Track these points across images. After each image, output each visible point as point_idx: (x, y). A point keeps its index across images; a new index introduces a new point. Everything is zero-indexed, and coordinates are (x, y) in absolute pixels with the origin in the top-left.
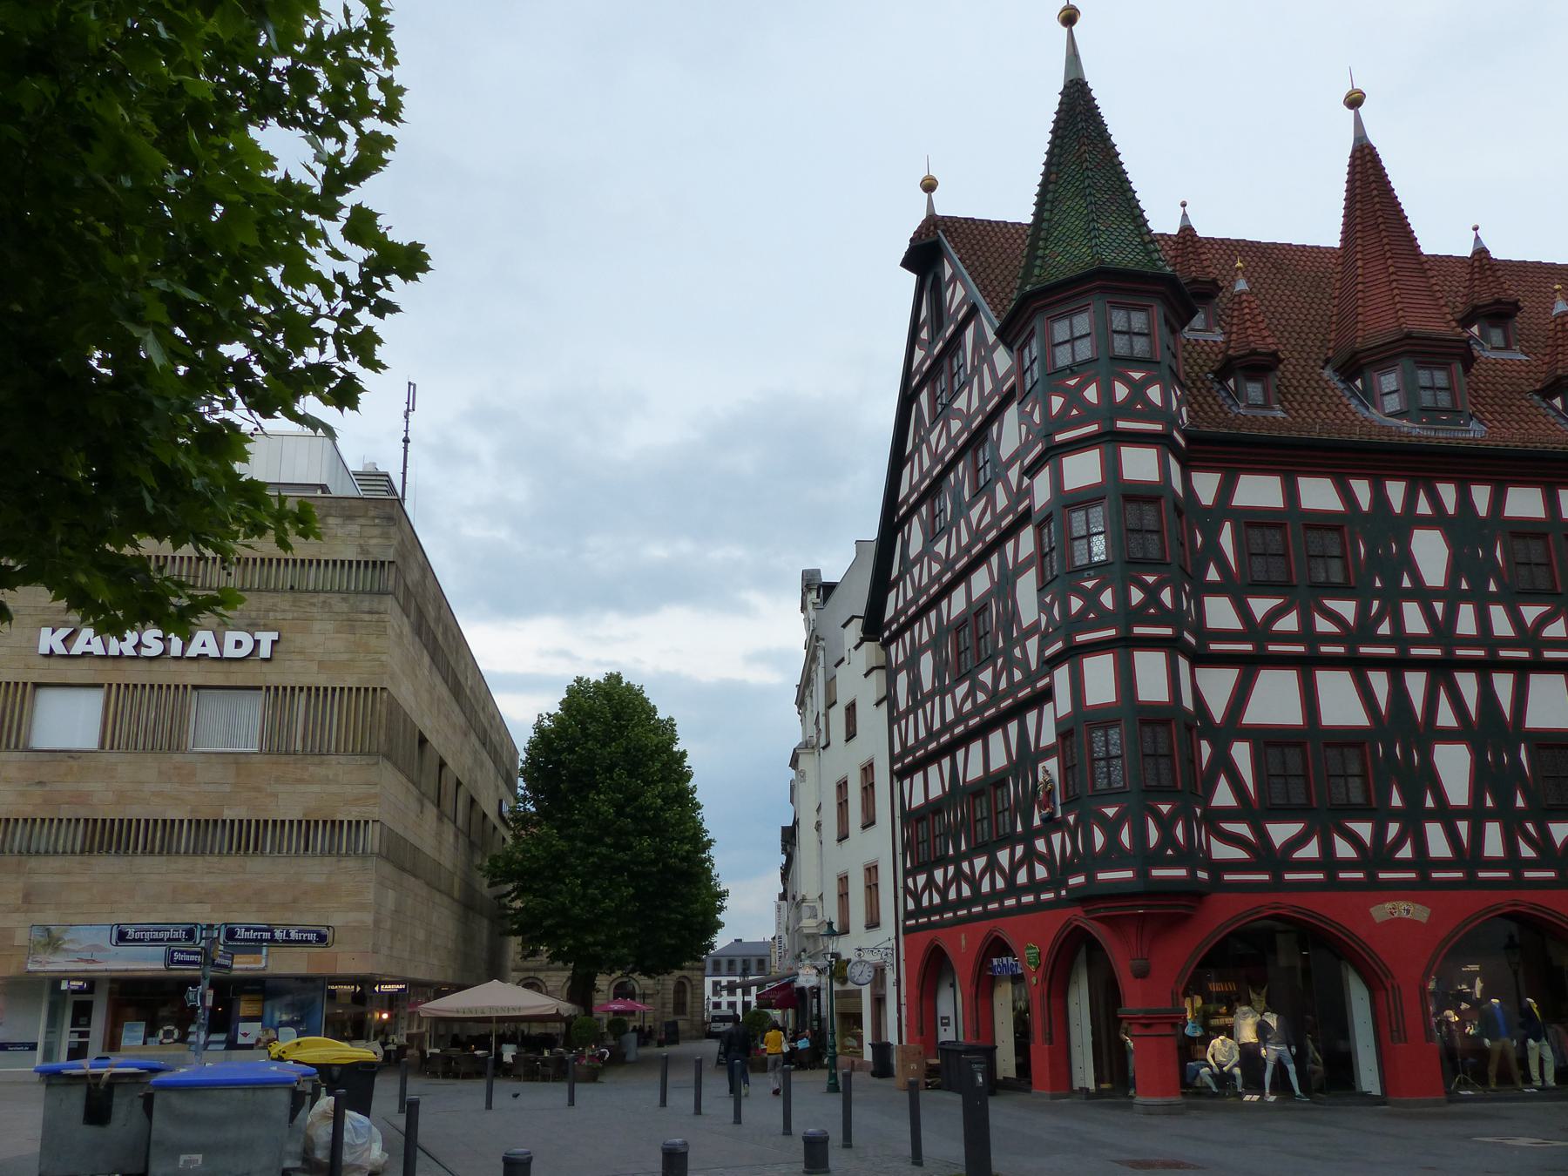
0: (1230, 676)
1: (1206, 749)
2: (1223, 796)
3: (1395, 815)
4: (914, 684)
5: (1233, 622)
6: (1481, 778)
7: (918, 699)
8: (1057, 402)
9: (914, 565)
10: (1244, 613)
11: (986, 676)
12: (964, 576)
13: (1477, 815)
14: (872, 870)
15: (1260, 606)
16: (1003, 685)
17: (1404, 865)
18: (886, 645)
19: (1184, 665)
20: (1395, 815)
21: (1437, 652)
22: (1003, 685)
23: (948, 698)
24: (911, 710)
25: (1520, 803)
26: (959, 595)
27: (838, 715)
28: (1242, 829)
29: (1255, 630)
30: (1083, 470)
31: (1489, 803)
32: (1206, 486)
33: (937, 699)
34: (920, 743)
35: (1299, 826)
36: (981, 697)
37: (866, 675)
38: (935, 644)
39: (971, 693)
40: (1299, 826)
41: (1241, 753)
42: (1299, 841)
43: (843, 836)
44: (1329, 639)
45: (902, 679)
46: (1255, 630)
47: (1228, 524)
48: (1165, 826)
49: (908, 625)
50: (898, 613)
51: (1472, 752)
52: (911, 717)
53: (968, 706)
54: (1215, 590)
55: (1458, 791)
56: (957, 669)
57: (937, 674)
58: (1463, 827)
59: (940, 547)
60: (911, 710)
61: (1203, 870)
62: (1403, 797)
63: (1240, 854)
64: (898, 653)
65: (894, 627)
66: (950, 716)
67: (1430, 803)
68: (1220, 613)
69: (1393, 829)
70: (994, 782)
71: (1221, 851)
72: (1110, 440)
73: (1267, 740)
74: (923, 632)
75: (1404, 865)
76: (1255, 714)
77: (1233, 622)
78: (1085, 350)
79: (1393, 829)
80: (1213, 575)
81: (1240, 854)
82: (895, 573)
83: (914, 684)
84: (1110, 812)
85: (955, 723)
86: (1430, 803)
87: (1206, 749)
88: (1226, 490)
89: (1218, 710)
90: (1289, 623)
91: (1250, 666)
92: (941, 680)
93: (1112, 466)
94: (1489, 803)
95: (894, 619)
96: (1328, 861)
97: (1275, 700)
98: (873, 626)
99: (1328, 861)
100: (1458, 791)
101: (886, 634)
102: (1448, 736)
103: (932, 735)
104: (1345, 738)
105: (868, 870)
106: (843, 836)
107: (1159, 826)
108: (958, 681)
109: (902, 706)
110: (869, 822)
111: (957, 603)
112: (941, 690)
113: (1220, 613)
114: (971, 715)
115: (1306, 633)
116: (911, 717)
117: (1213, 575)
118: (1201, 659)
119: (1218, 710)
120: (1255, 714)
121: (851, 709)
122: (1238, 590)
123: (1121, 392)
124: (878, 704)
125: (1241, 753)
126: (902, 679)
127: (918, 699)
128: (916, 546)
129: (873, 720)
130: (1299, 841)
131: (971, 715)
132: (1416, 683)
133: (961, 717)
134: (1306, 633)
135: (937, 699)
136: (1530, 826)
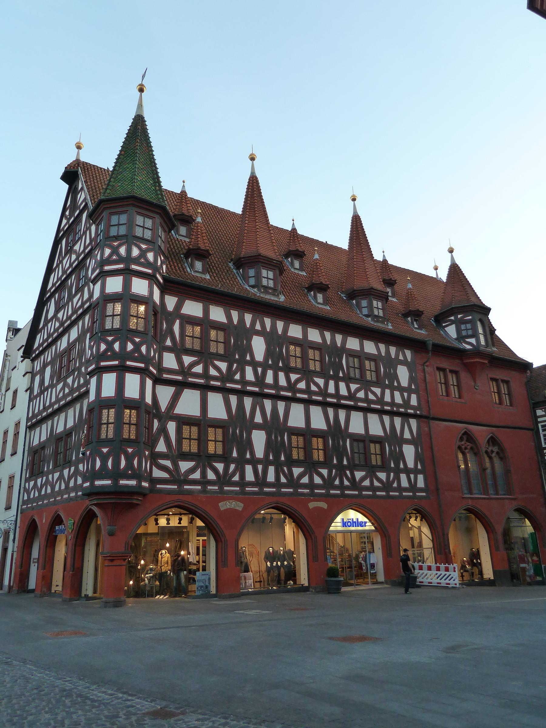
0: (171, 390)
2: (161, 447)
4: (42, 381)
7: (43, 390)
8: (108, 251)
9: (49, 322)
10: (180, 361)
11: (70, 380)
12: (67, 330)
13: (266, 463)
16: (76, 385)
18: (33, 360)
19: (149, 383)
21: (257, 389)
22: (76, 385)
23: (54, 389)
24: (42, 392)
25: (283, 458)
26: (65, 339)
27: (10, 394)
28: (168, 463)
29: (184, 371)
30: (114, 285)
31: (271, 458)
32: (171, 302)
33: (50, 390)
34: (40, 412)
36: (67, 390)
37: (24, 376)
38: (52, 363)
39: (63, 389)
41: (172, 427)
44: (215, 378)
45: (37, 379)
49: (42, 353)
50: (40, 345)
52: (38, 398)
53: (61, 395)
54: (169, 350)
56: (59, 376)
57: (52, 378)
58: (260, 467)
59: (60, 315)
60: (42, 392)
61: (145, 481)
63: (165, 475)
64: (38, 365)
65: (37, 352)
66: (53, 399)
68: (170, 361)
70: (68, 434)
71: (157, 473)
72: (128, 274)
73: (184, 421)
74: (48, 356)
75: (235, 484)
76: (179, 410)
80: (168, 343)
81: (165, 475)
82: (41, 325)
83: (42, 381)
85: (55, 403)
87: (156, 423)
90: (199, 369)
92: (53, 381)
93: (127, 285)
94: (271, 458)
95: (38, 348)
98: (28, 352)
101: (34, 355)
102: (258, 427)
103: (45, 408)
104: (216, 424)
108: (58, 382)
109: (35, 393)
111: (63, 344)
112: (52, 386)
113: (170, 361)
114: (62, 399)
115: (205, 375)
116: (38, 398)
117: (168, 343)
118: (158, 381)
120: (179, 410)
121: (15, 392)
122: (179, 350)
123: (135, 252)
124: (26, 391)
125: (172, 427)
126: (37, 379)
127: (43, 390)
128: (51, 314)
129: (23, 398)
131: (62, 399)
132: (248, 402)
133: (58, 400)
134: (205, 375)
135: (50, 390)
136: (285, 469)
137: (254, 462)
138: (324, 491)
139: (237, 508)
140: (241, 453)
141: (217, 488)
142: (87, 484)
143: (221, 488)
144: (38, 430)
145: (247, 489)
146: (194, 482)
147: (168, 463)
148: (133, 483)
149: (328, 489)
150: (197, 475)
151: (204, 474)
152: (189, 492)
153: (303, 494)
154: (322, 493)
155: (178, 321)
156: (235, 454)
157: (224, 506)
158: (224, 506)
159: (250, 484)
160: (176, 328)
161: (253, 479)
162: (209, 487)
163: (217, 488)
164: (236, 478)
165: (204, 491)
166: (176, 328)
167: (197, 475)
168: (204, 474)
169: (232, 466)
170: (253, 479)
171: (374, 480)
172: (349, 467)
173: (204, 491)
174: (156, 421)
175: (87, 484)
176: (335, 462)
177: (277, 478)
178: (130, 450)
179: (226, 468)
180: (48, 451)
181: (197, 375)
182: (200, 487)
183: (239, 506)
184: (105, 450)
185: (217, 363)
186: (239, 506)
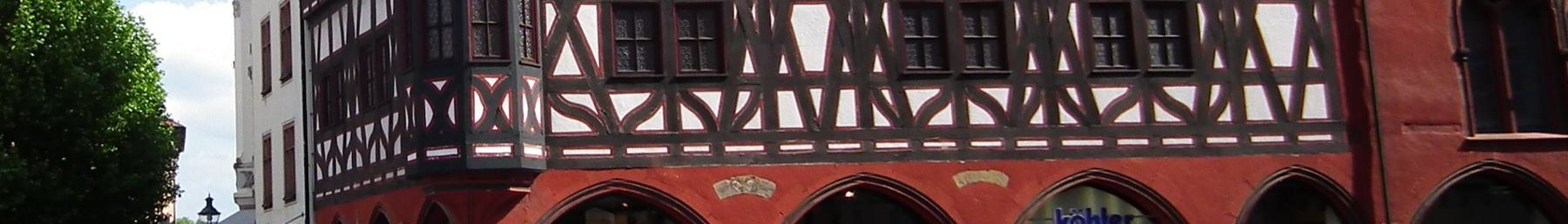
1: (551, 13)
2: (567, 65)
3: (747, 83)
6: (840, 39)
14: (289, 131)
17: (753, 137)
20: (747, 83)
35: (646, 96)
40: (646, 96)
42: (644, 112)
43: (267, 90)
48: (492, 102)
51: (832, 10)
55: (814, 56)
62: (756, 63)
63: (583, 127)
69: (744, 97)
71: (563, 124)
81: (583, 127)
84: (440, 85)
86: (783, 69)
96: (674, 135)
99: (674, 135)
100: (814, 56)
105: (285, 131)
106: (267, 90)
107: (486, 101)
110: (286, 76)
130: (644, 112)
137: (800, 82)
138: (998, 144)
139: (761, 193)
140: (766, 65)
141: (706, 149)
142: (412, 157)
143: (717, 149)
144: (325, 23)
145: (783, 147)
146: (650, 139)
147: (585, 100)
148: (505, 150)
149: (1011, 138)
150: (656, 122)
151: (673, 120)
152: (642, 163)
153: (937, 153)
154: (992, 150)
156: (748, 68)
157: (724, 189)
158: (724, 189)
159: (793, 135)
161: (799, 124)
162: (687, 149)
163: (706, 149)
164: (755, 123)
165: (676, 157)
167: (656, 122)
168: (673, 120)
170: (799, 124)
171: (1062, 110)
172: (1070, 79)
173: (676, 157)
174: (550, 8)
175: (412, 157)
176: (1032, 66)
177: (865, 117)
178: (492, 81)
179: (729, 103)
180: (350, 75)
182: (665, 150)
183: (766, 189)
184: (440, 85)
186: (766, 189)
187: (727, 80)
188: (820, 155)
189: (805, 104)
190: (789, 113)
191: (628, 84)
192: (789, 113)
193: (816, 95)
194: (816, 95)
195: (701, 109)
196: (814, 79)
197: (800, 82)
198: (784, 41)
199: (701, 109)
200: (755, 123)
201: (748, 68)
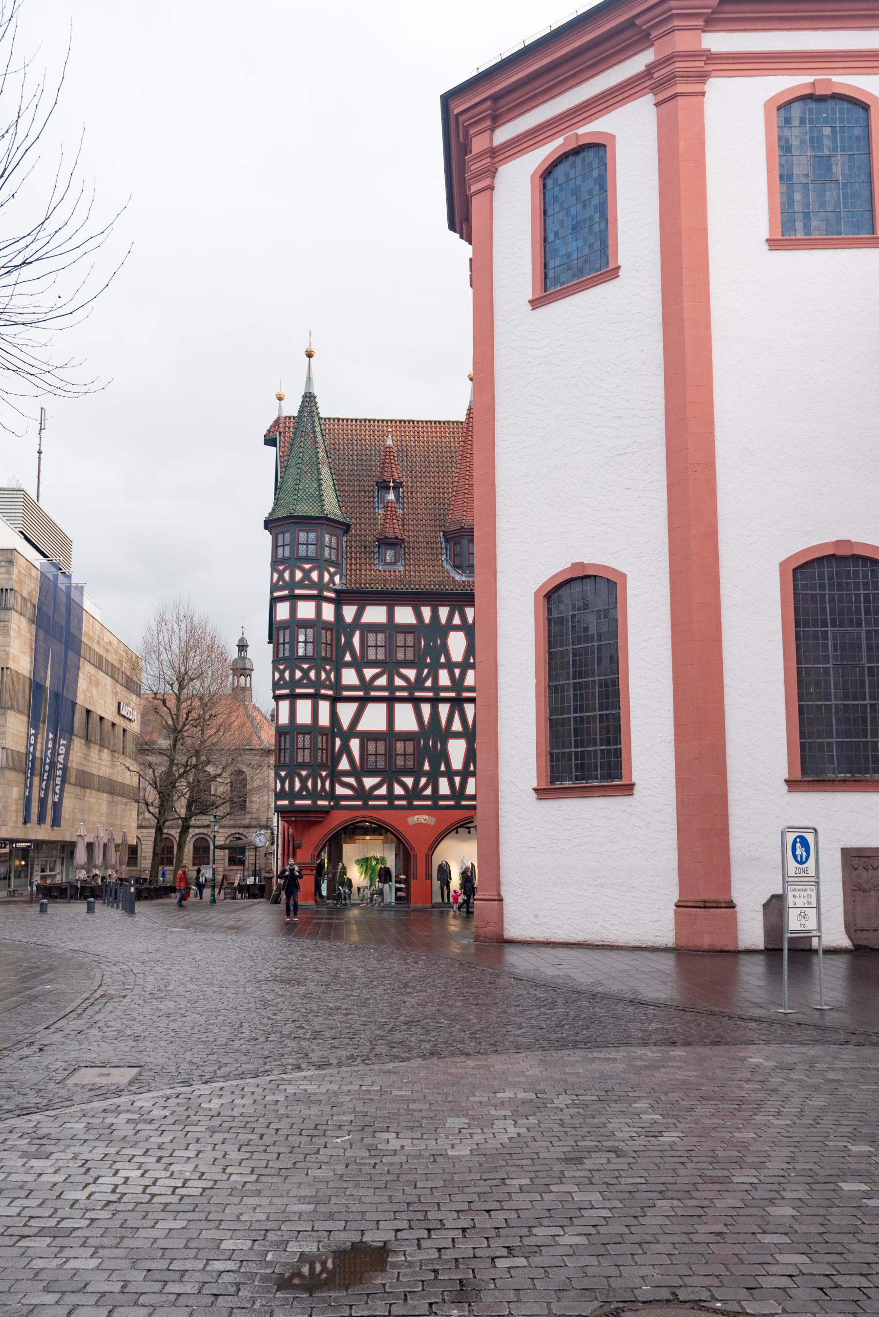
0: (353, 707)
3: (425, 774)
5: (355, 681)
10: (361, 676)
15: (369, 673)
20: (425, 774)
29: (365, 685)
32: (349, 612)
41: (355, 744)
42: (378, 786)
46: (365, 685)
47: (358, 633)
54: (348, 665)
67: (443, 768)
68: (349, 677)
73: (367, 737)
76: (364, 725)
77: (355, 681)
78: (312, 551)
79: (423, 780)
80: (348, 658)
86: (443, 768)
87: (338, 742)
88: (359, 614)
89: (345, 723)
91: (363, 701)
97: (374, 718)
113: (349, 677)
117: (348, 658)
119: (345, 723)
120: (362, 726)
122: (359, 665)
125: (355, 744)
130: (378, 786)
155: (358, 633)
160: (356, 640)
166: (356, 640)
169: (423, 780)
181: (380, 688)
185: (404, 671)
187: (416, 773)
188: (458, 807)
189: (452, 784)
190: (444, 787)
191: (372, 773)
192: (444, 787)
193: (457, 780)
194: (457, 780)
195: (404, 785)
196: (457, 773)
197: (450, 774)
198: (445, 756)
199: (404, 785)
200: (428, 792)
201: (427, 767)
